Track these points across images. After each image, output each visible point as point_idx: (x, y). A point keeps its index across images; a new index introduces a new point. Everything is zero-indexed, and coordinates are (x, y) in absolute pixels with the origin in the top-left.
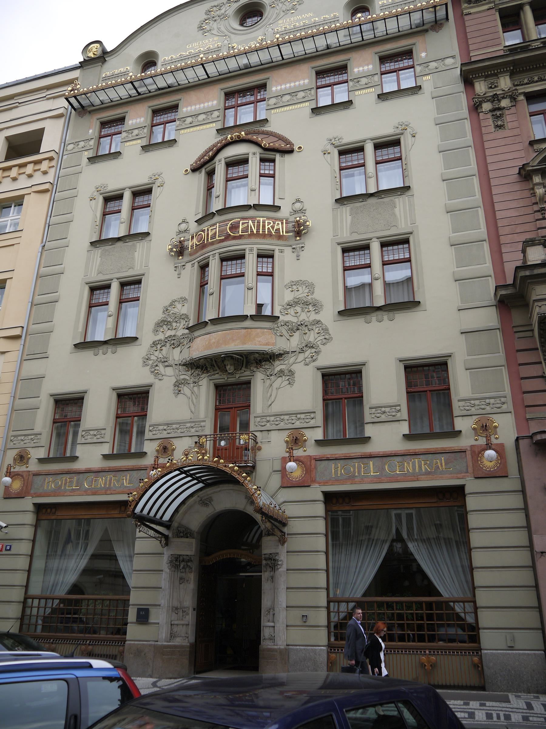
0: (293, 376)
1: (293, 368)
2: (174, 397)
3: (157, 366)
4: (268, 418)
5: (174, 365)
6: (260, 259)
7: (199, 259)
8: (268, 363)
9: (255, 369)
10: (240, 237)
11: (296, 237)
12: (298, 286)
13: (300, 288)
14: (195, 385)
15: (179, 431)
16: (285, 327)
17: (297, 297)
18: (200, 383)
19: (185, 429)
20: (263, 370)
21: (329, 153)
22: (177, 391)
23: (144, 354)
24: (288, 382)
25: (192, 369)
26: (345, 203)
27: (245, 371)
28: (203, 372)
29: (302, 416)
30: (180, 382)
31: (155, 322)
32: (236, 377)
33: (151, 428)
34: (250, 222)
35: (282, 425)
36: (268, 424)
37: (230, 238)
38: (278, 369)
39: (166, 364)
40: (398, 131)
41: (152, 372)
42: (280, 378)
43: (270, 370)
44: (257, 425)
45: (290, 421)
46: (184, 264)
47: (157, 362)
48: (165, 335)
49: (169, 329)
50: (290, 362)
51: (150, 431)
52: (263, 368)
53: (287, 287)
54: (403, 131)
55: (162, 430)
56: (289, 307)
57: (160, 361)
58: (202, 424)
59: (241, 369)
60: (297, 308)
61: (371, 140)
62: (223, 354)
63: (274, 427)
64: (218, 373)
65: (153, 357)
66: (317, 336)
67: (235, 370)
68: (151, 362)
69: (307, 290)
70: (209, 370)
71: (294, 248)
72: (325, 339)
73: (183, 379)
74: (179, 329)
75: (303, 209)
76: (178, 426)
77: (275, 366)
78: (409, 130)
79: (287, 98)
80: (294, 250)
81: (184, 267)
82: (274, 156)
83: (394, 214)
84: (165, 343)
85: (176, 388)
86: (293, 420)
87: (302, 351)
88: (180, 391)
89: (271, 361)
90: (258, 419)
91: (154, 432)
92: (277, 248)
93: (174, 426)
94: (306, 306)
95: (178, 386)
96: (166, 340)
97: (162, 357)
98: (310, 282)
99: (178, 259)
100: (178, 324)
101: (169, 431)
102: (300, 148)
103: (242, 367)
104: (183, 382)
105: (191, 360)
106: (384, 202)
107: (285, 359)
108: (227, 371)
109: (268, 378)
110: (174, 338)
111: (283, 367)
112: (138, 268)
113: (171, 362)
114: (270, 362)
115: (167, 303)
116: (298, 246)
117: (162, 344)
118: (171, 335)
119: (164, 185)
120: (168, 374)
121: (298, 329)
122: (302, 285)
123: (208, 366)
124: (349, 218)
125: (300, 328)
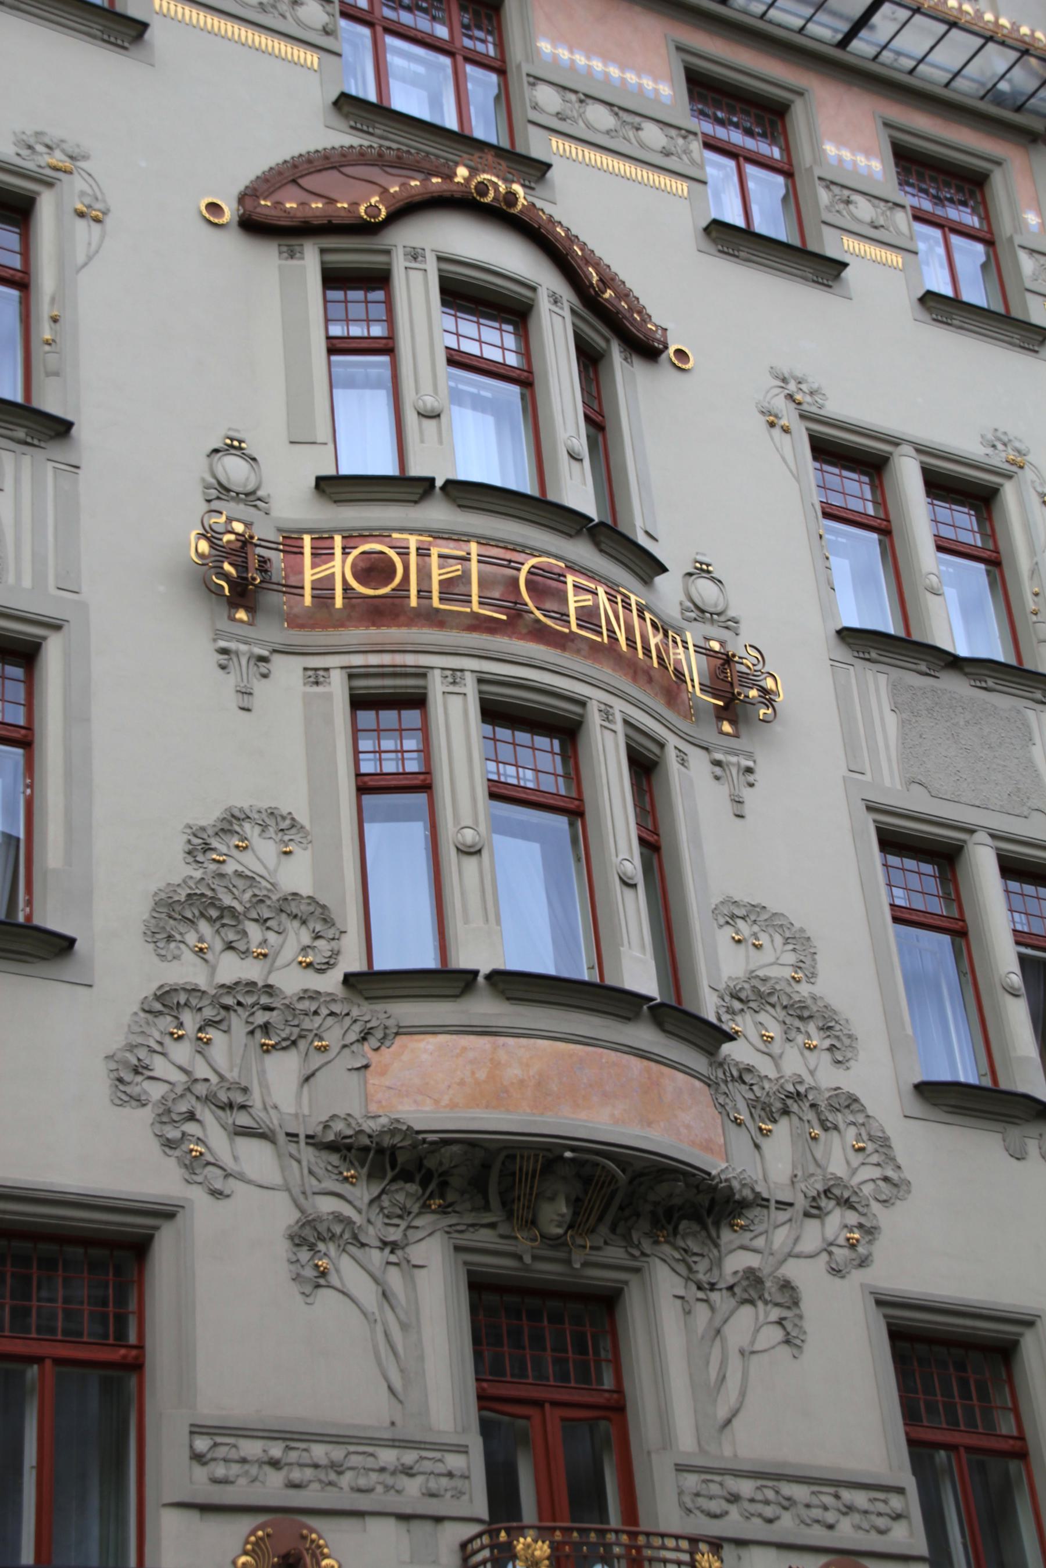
0: (797, 1312)
1: (792, 1270)
2: (300, 1298)
3: (191, 1116)
4: (734, 1484)
5: (282, 1138)
6: (367, 717)
7: (357, 660)
8: (696, 1227)
9: (647, 1246)
10: (562, 641)
11: (720, 718)
12: (756, 928)
13: (764, 939)
14: (393, 1258)
15: (346, 1480)
16: (744, 1088)
17: (761, 973)
18: (417, 1253)
19: (374, 1476)
20: (677, 1256)
21: (786, 430)
22: (309, 1273)
23: (116, 1042)
24: (778, 1334)
25: (370, 1176)
26: (874, 655)
27: (606, 1243)
28: (425, 1208)
29: (860, 1499)
30: (322, 1228)
31: (153, 888)
32: (568, 1262)
33: (202, 1444)
34: (601, 591)
35: (787, 1526)
36: (734, 1512)
37: (524, 631)
38: (736, 1262)
39: (243, 1119)
40: (997, 460)
41: (169, 1144)
42: (747, 1310)
43: (702, 1266)
44: (690, 1505)
45: (816, 1513)
46: (265, 653)
47: (193, 1100)
48: (213, 969)
49: (230, 947)
50: (776, 1246)
51: (198, 1458)
52: (676, 1248)
53: (722, 921)
54: (1014, 468)
55: (261, 1463)
56: (737, 1005)
57: (209, 1099)
58: (455, 1462)
59: (593, 1231)
60: (762, 1017)
61: (918, 451)
62: (573, 1149)
63: (755, 1529)
64: (492, 1226)
65: (160, 1067)
66: (856, 1159)
67: (570, 1227)
68: (156, 1091)
69: (790, 958)
70: (451, 1197)
71: (718, 763)
72: (886, 1179)
73: (339, 1218)
74: (280, 962)
75: (731, 613)
76: (337, 1453)
77: (723, 1249)
78: (1028, 474)
79: (600, 117)
80: (718, 771)
81: (263, 667)
82: (602, 343)
83: (1030, 765)
84: (223, 1013)
85: (304, 1255)
86: (826, 1508)
87: (814, 1211)
88: (323, 1274)
89: (709, 1221)
90: (692, 1481)
91: (220, 1471)
92: (672, 741)
93: (319, 1452)
94: (797, 1023)
95: (312, 1247)
96: (229, 1001)
97: (214, 1079)
98: (797, 925)
99: (233, 619)
100: (272, 937)
101: (296, 1475)
102: (680, 353)
103: (600, 1219)
104: (337, 1229)
105: (393, 1132)
106: (996, 708)
107: (759, 1228)
108: (534, 1223)
109: (701, 1295)
110: (264, 1000)
111: (752, 1260)
112: (27, 583)
113: (259, 1115)
114: (705, 1227)
115: (209, 817)
116: (733, 759)
117: (209, 1013)
118: (254, 984)
119: (109, 221)
120: (251, 1173)
121: (786, 1112)
122: (771, 930)
123: (455, 1181)
124: (892, 720)
125: (794, 1107)
